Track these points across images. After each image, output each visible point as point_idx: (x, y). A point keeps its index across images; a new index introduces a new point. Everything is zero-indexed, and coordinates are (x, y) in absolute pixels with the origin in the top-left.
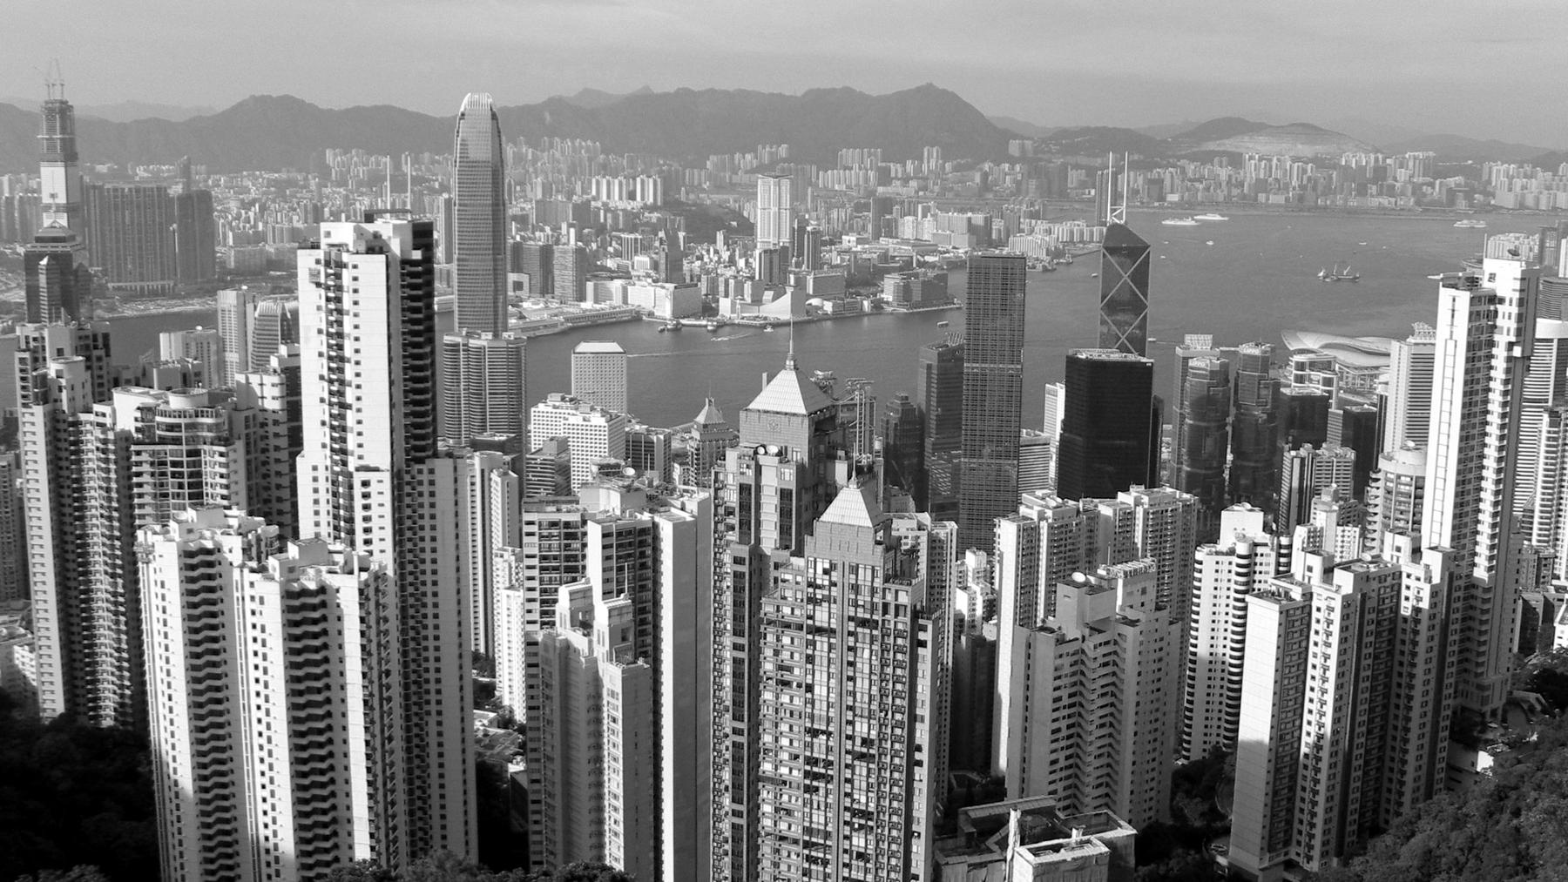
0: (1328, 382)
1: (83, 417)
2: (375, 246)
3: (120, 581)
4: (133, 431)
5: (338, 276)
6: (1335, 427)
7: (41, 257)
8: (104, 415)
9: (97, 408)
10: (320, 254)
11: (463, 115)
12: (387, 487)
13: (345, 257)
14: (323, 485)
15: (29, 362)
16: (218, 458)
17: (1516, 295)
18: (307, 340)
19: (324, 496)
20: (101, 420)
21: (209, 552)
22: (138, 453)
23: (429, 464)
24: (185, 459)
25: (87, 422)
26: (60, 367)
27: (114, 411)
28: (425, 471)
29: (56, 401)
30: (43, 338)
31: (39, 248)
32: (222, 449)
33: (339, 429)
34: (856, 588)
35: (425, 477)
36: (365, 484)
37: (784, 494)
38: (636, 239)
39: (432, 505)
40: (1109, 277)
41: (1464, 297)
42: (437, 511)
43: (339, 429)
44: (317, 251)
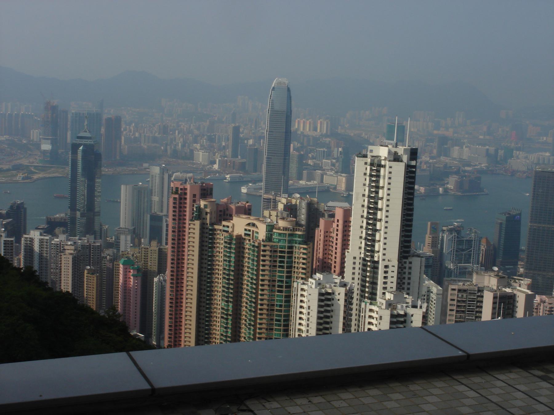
1: (216, 227)
2: (396, 158)
4: (243, 235)
5: (378, 171)
7: (80, 145)
8: (228, 227)
9: (224, 223)
10: (369, 160)
11: (274, 88)
13: (383, 163)
14: (357, 266)
15: (178, 199)
16: (302, 250)
18: (357, 199)
19: (357, 271)
20: (226, 229)
21: (329, 294)
22: (264, 246)
23: (410, 259)
24: (286, 250)
25: (218, 230)
26: (206, 203)
27: (233, 225)
28: (408, 263)
29: (204, 219)
30: (186, 189)
31: (78, 141)
32: (305, 246)
33: (371, 241)
35: (407, 265)
36: (386, 267)
38: (324, 151)
39: (409, 278)
42: (411, 281)
43: (371, 241)
44: (365, 160)
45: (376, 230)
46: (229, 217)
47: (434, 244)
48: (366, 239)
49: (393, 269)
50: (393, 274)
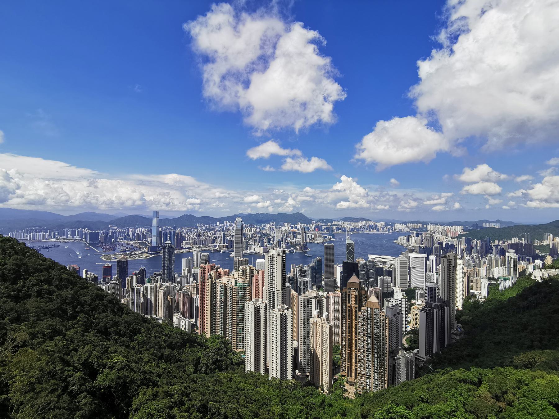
0: (381, 264)
1: (217, 281)
3: (223, 310)
5: (273, 259)
6: (384, 273)
12: (281, 294)
17: (454, 259)
33: (271, 284)
34: (375, 312)
35: (285, 292)
36: (278, 293)
37: (356, 296)
40: (348, 248)
41: (446, 260)
43: (271, 284)
44: (268, 255)
45: (273, 288)
46: (220, 277)
47: (294, 272)
48: (270, 283)
49: (280, 294)
50: (280, 296)
